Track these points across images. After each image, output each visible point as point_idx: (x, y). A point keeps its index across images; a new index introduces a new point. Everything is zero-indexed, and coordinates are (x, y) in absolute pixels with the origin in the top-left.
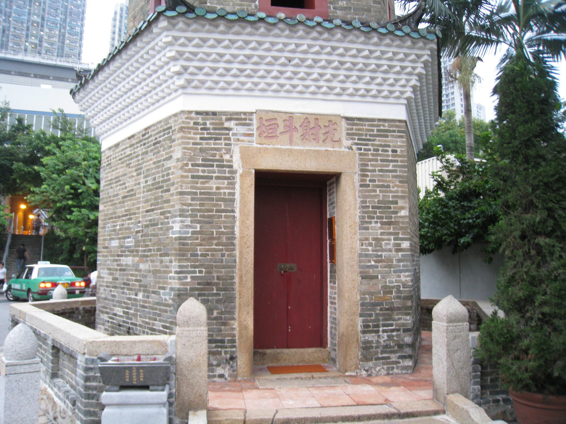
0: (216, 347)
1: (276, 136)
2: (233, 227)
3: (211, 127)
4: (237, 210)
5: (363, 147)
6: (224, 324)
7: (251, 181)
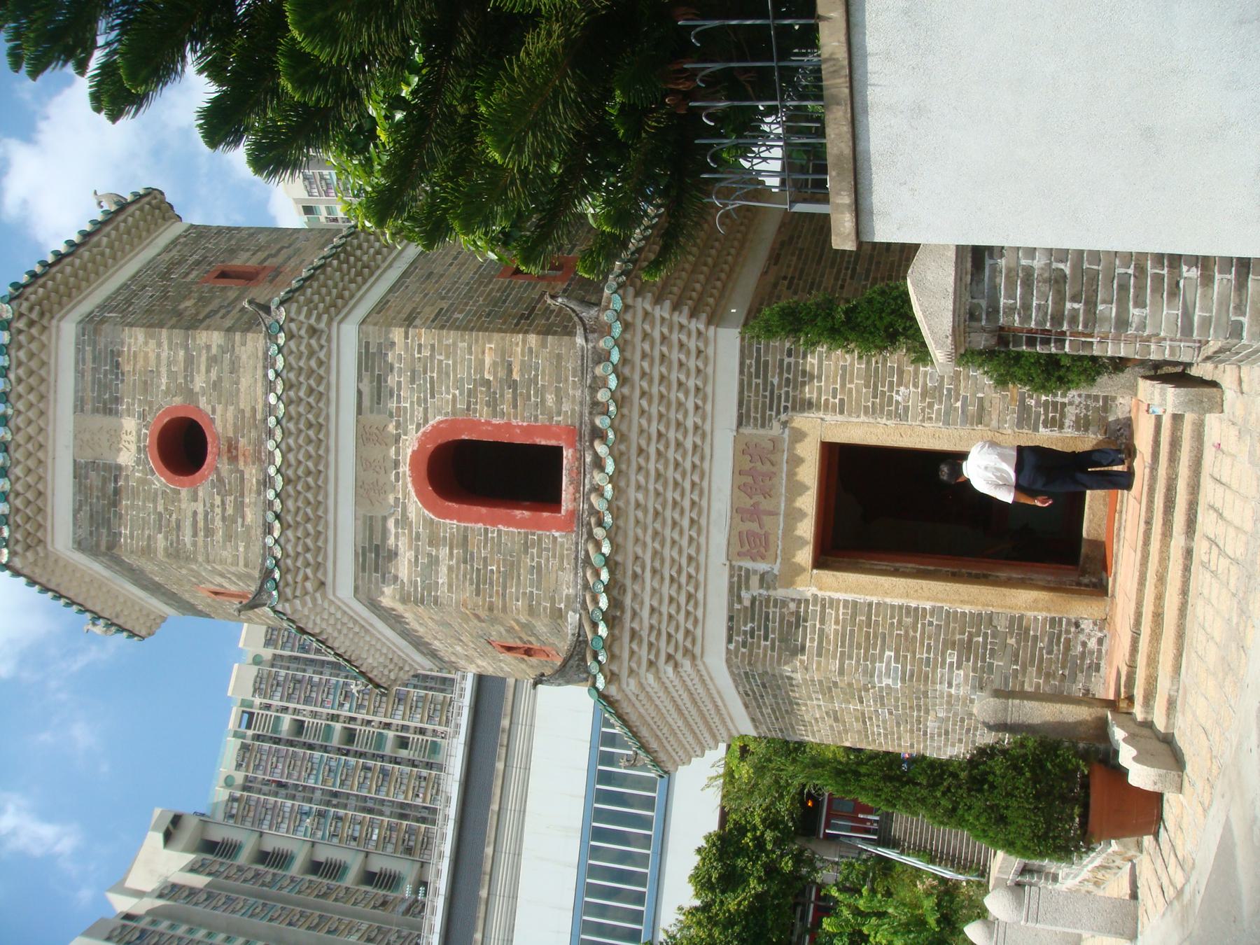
0: (1058, 645)
1: (766, 536)
2: (893, 607)
3: (749, 625)
4: (869, 599)
5: (783, 404)
6: (1027, 630)
7: (827, 576)
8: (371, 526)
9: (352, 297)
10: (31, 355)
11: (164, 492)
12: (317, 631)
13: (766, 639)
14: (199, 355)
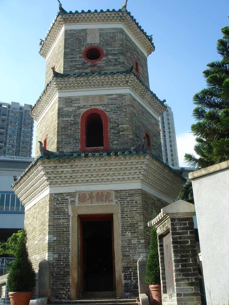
0: (62, 286)
1: (86, 201)
3: (60, 199)
4: (71, 231)
5: (122, 202)
7: (76, 218)
8: (77, 100)
9: (136, 92)
10: (113, 17)
12: (48, 90)
13: (56, 204)
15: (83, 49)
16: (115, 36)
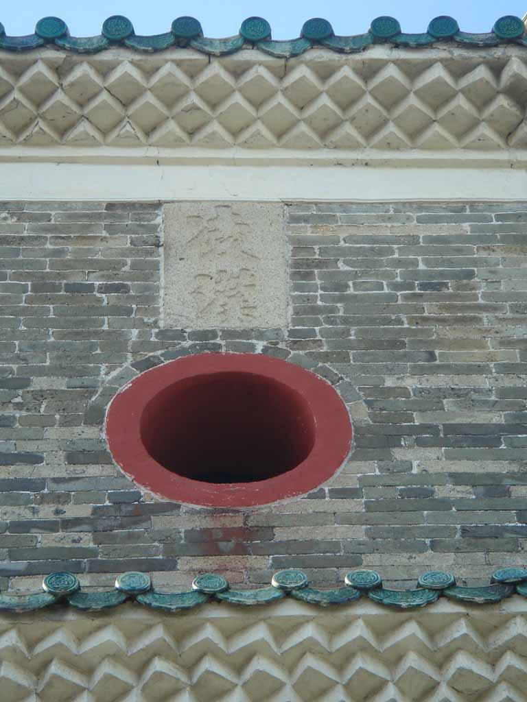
10: (438, 99)
11: (90, 390)
14: (498, 457)
15: (115, 376)
16: (454, 276)
